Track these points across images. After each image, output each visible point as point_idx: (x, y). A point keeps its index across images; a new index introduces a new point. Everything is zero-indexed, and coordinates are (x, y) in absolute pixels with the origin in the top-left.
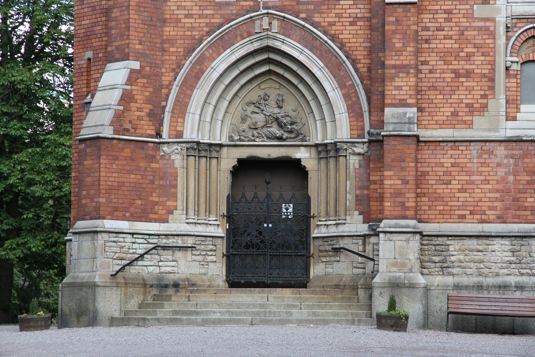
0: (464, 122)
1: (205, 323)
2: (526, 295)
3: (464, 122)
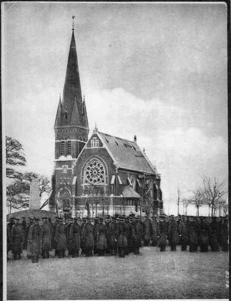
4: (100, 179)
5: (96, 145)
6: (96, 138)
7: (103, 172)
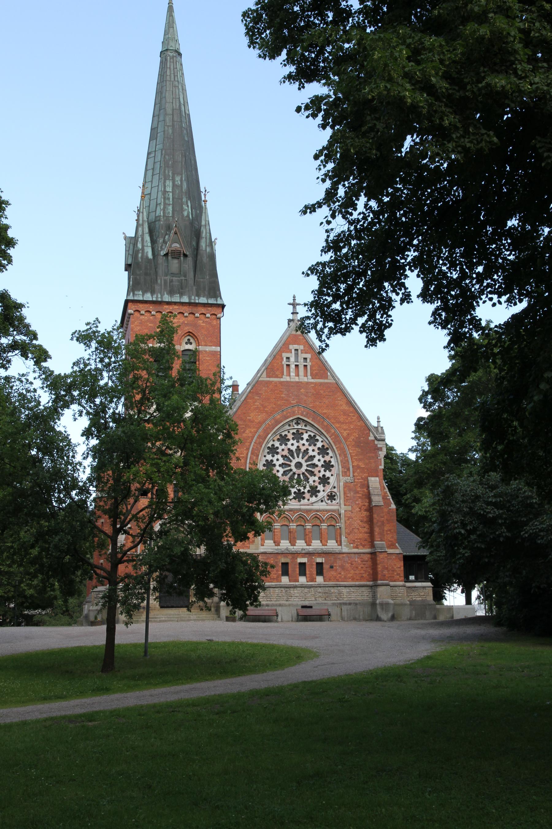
0: (247, 547)
1: (160, 621)
2: (269, 608)
3: (247, 547)
4: (320, 487)
5: (301, 369)
6: (301, 347)
7: (328, 466)
